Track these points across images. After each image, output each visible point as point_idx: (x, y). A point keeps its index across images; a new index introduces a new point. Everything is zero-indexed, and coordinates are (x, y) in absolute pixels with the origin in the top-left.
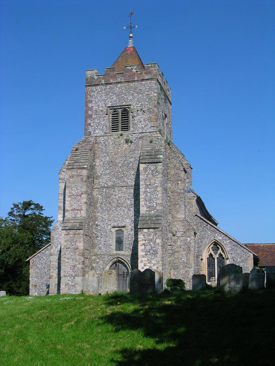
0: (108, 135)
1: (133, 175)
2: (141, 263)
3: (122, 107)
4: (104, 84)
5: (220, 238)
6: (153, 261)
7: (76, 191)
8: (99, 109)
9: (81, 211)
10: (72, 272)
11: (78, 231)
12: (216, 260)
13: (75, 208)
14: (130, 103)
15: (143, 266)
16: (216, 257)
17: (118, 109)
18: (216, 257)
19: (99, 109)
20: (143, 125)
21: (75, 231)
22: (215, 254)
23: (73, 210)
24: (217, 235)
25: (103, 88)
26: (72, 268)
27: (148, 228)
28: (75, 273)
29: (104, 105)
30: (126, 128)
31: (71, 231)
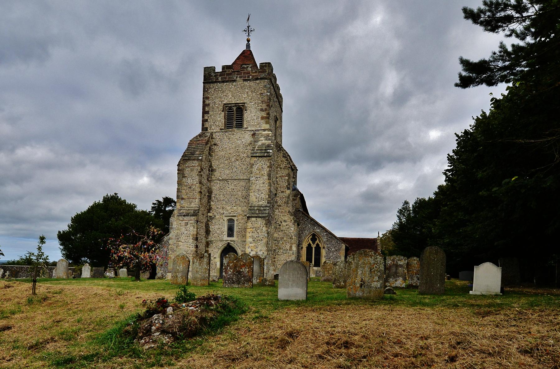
0: (223, 131)
1: (245, 169)
3: (237, 105)
4: (221, 81)
5: (319, 230)
6: (259, 247)
12: (314, 249)
14: (245, 102)
15: (250, 251)
16: (314, 246)
17: (234, 106)
18: (314, 246)
20: (255, 123)
22: (314, 243)
23: (189, 198)
24: (316, 228)
27: (256, 217)
29: (220, 102)
30: (240, 125)
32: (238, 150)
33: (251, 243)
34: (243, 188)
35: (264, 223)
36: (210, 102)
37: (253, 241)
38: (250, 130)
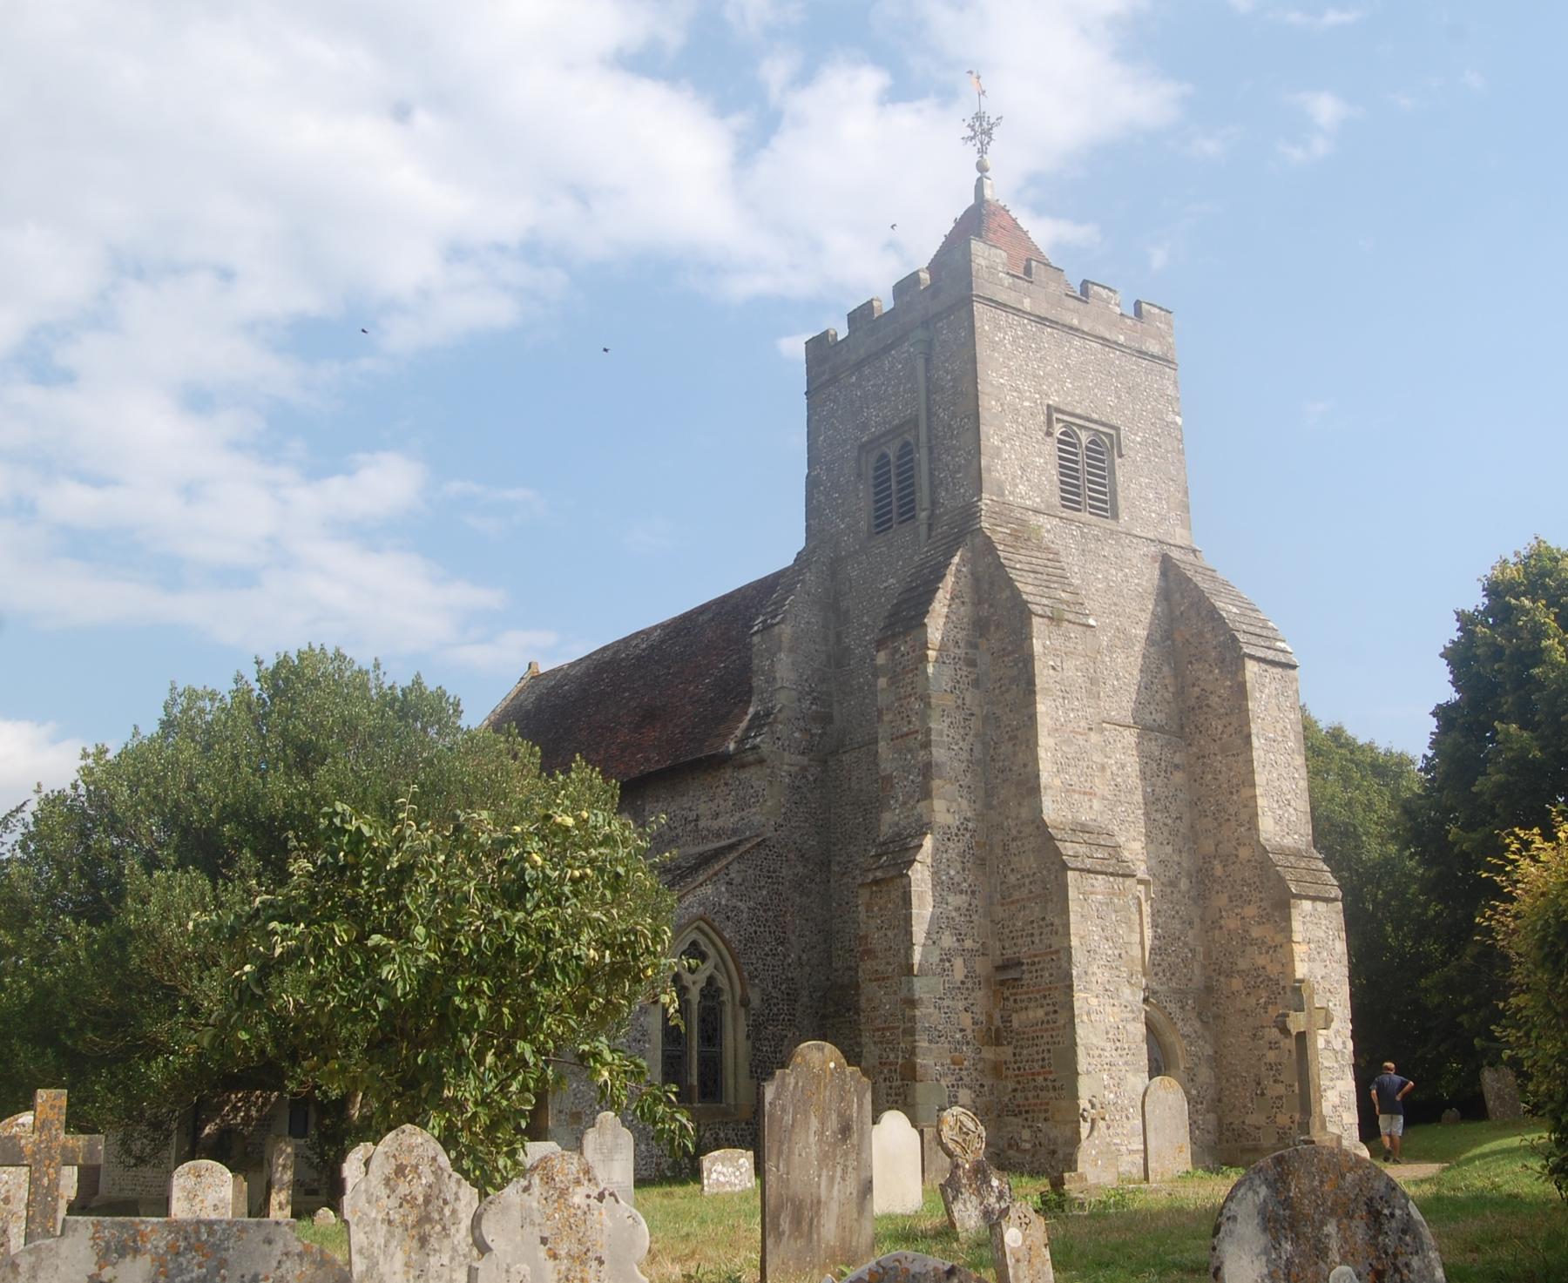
7: (1072, 715)
9: (1090, 800)
10: (1114, 1053)
11: (1121, 879)
17: (1081, 427)
20: (1153, 515)
21: (1111, 879)
23: (1068, 791)
25: (1029, 327)
26: (1110, 1036)
27: (1314, 899)
28: (1121, 1056)
31: (1100, 877)
32: (1115, 604)
36: (1001, 381)
38: (1147, 539)
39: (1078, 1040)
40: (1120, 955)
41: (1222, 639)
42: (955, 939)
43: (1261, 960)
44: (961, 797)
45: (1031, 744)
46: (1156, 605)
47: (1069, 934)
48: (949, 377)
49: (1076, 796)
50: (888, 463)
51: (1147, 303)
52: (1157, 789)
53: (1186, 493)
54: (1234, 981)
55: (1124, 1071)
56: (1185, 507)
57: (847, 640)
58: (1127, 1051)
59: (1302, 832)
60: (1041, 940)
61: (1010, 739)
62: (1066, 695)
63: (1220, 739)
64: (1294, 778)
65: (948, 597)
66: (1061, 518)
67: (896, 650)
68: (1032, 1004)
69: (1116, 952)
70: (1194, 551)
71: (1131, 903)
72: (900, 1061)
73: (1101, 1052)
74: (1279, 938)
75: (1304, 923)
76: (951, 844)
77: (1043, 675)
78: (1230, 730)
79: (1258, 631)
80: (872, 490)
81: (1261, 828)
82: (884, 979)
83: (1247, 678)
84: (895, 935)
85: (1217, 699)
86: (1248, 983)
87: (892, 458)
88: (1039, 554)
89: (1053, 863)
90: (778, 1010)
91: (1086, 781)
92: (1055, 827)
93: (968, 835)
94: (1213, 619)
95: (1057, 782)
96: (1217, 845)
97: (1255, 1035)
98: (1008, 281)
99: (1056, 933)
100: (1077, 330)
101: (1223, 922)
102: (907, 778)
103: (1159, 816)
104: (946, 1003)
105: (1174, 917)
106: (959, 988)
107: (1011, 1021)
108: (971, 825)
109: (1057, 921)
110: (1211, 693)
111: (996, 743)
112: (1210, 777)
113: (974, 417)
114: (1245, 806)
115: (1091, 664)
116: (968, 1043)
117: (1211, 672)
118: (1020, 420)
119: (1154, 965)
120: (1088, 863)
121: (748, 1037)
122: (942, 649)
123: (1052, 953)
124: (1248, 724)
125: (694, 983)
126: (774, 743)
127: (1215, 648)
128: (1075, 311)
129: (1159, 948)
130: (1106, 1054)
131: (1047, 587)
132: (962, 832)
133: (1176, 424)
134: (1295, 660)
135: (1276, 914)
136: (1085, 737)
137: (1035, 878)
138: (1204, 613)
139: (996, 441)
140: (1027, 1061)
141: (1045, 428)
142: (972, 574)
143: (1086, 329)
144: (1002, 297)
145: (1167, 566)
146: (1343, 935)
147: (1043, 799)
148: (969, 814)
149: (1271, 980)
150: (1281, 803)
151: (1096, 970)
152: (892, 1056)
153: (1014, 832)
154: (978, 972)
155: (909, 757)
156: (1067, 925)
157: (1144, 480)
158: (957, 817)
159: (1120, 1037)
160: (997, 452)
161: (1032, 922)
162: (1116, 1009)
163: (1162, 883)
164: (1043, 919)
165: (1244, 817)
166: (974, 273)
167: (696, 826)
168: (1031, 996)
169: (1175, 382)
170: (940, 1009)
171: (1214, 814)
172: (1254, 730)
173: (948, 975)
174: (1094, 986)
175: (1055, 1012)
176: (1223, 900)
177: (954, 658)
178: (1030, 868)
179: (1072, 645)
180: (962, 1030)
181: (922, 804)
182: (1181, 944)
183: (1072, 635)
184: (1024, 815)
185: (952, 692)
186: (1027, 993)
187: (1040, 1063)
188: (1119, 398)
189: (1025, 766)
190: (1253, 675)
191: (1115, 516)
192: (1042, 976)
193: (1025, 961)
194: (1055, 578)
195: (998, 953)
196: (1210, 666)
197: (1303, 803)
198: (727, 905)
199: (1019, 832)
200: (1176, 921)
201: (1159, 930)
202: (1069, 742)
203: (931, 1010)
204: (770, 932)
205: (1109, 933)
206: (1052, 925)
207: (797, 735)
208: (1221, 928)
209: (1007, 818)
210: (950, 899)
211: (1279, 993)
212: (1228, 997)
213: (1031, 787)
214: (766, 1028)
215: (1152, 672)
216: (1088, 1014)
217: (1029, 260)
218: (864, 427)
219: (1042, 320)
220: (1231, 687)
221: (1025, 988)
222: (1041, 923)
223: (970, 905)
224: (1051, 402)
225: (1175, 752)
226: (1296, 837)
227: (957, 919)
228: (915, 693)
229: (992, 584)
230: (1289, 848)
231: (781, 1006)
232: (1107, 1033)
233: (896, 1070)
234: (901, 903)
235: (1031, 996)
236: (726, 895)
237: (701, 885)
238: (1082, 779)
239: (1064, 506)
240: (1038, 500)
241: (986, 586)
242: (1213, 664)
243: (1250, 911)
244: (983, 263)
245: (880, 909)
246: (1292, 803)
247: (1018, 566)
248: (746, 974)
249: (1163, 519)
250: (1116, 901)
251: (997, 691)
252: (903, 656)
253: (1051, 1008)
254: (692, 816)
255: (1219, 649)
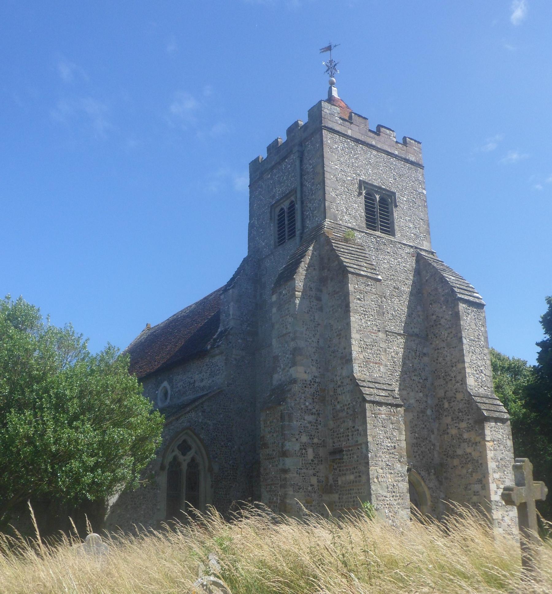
2: (493, 483)
7: (369, 324)
8: (348, 178)
9: (379, 367)
10: (391, 498)
13: (369, 359)
15: (496, 489)
19: (348, 178)
20: (412, 235)
26: (389, 489)
28: (395, 500)
33: (495, 472)
34: (414, 354)
35: (506, 432)
36: (336, 167)
37: (496, 468)
39: (372, 492)
40: (395, 446)
41: (447, 291)
42: (308, 437)
43: (468, 450)
44: (313, 365)
45: (348, 338)
46: (414, 277)
47: (367, 435)
48: (311, 167)
49: (371, 364)
50: (284, 211)
51: (409, 138)
52: (415, 365)
53: (428, 225)
54: (455, 460)
55: (397, 508)
56: (428, 233)
57: (265, 297)
58: (399, 497)
59: (489, 386)
60: (352, 439)
61: (337, 335)
62: (366, 313)
63: (446, 340)
64: (484, 359)
65: (307, 266)
66: (366, 233)
67: (281, 293)
68: (349, 472)
69: (393, 445)
70: (432, 253)
71: (400, 419)
72: (279, 501)
73: (385, 498)
74: (478, 439)
75: (491, 431)
76: (307, 389)
77: (354, 303)
78: (451, 335)
79: (465, 288)
80: (277, 226)
81: (468, 383)
82: (271, 459)
83: (460, 310)
84: (277, 436)
85: (444, 321)
86: (462, 461)
87: (286, 210)
88: (353, 246)
89: (358, 398)
90: (228, 473)
91: (377, 357)
92: (360, 380)
93: (316, 385)
94: (442, 282)
95: (361, 356)
96: (445, 393)
97: (466, 488)
98: (340, 121)
99: (360, 435)
100: (374, 146)
101: (449, 431)
102: (285, 356)
103: (415, 378)
104: (303, 471)
105: (424, 428)
106: (310, 463)
107: (337, 481)
108: (317, 380)
109: (360, 428)
110: (442, 318)
111: (330, 338)
112: (441, 359)
113: (323, 183)
114: (460, 373)
115: (380, 298)
116: (315, 492)
117: (441, 307)
118: (346, 186)
119: (414, 452)
120: (377, 399)
121: (212, 487)
122: (304, 292)
123: (358, 445)
124: (460, 332)
125: (184, 460)
126: (228, 344)
127: (443, 296)
128: (374, 138)
129: (417, 444)
130: (387, 499)
131: (357, 260)
132: (313, 383)
133: (423, 193)
134: (483, 302)
135: (477, 426)
136: (376, 335)
137: (350, 406)
138: (437, 279)
139: (333, 194)
140: (346, 502)
141: (358, 190)
142: (320, 256)
143: (379, 146)
144: (337, 128)
145: (419, 258)
146: (511, 437)
147: (354, 365)
148: (316, 374)
149: (475, 460)
150: (478, 372)
151: (381, 454)
152: (275, 499)
153: (339, 383)
154: (320, 455)
155: (286, 346)
156: (365, 430)
157: (407, 218)
158: (310, 376)
159: (395, 490)
160: (334, 200)
161: (348, 429)
162: (392, 475)
163: (418, 411)
164: (354, 427)
165: (459, 378)
166: (323, 116)
167: (194, 385)
168: (347, 468)
169: (423, 175)
170: (300, 474)
171: (444, 377)
172: (464, 335)
173: (304, 457)
174: (380, 463)
175: (360, 476)
176: (448, 420)
177: (310, 296)
178: (347, 401)
179: (370, 289)
180: (312, 485)
181: (293, 369)
182: (428, 442)
183: (369, 283)
184: (344, 374)
185: (308, 313)
186: (345, 466)
187: (352, 503)
188: (395, 179)
189: (345, 348)
190: (463, 308)
191: (393, 235)
192: (353, 457)
193: (345, 449)
194: (361, 257)
195: (331, 445)
196: (441, 304)
197: (489, 372)
198: (202, 422)
199: (342, 383)
200: (426, 430)
201: (416, 435)
202: (368, 337)
203: (295, 475)
204: (224, 436)
205: (388, 435)
206: (358, 430)
207: (239, 341)
208: (448, 433)
209: (336, 376)
210: (306, 418)
211: (479, 467)
212: (452, 469)
213: (348, 360)
214: (221, 482)
215: (412, 308)
216: (377, 478)
217: (351, 113)
218: (274, 196)
219: (357, 141)
220: (451, 314)
221: (345, 464)
222: (353, 429)
223: (317, 420)
224: (361, 179)
225: (424, 347)
226: (486, 388)
227: (309, 428)
228: (289, 314)
229: (329, 259)
230: (482, 394)
231: (229, 472)
232: (388, 488)
233: (277, 506)
234: (280, 419)
235: (347, 468)
236: (202, 417)
237: (189, 412)
238: (374, 356)
239: (367, 228)
240: (354, 224)
241: (326, 261)
242: (442, 304)
243: (463, 425)
244: (328, 112)
245: (270, 423)
246: (483, 371)
247: (342, 250)
248: (211, 456)
249: (417, 236)
250: (392, 418)
251: (331, 313)
252: (284, 296)
253: (358, 474)
254: (192, 381)
255: (445, 296)
